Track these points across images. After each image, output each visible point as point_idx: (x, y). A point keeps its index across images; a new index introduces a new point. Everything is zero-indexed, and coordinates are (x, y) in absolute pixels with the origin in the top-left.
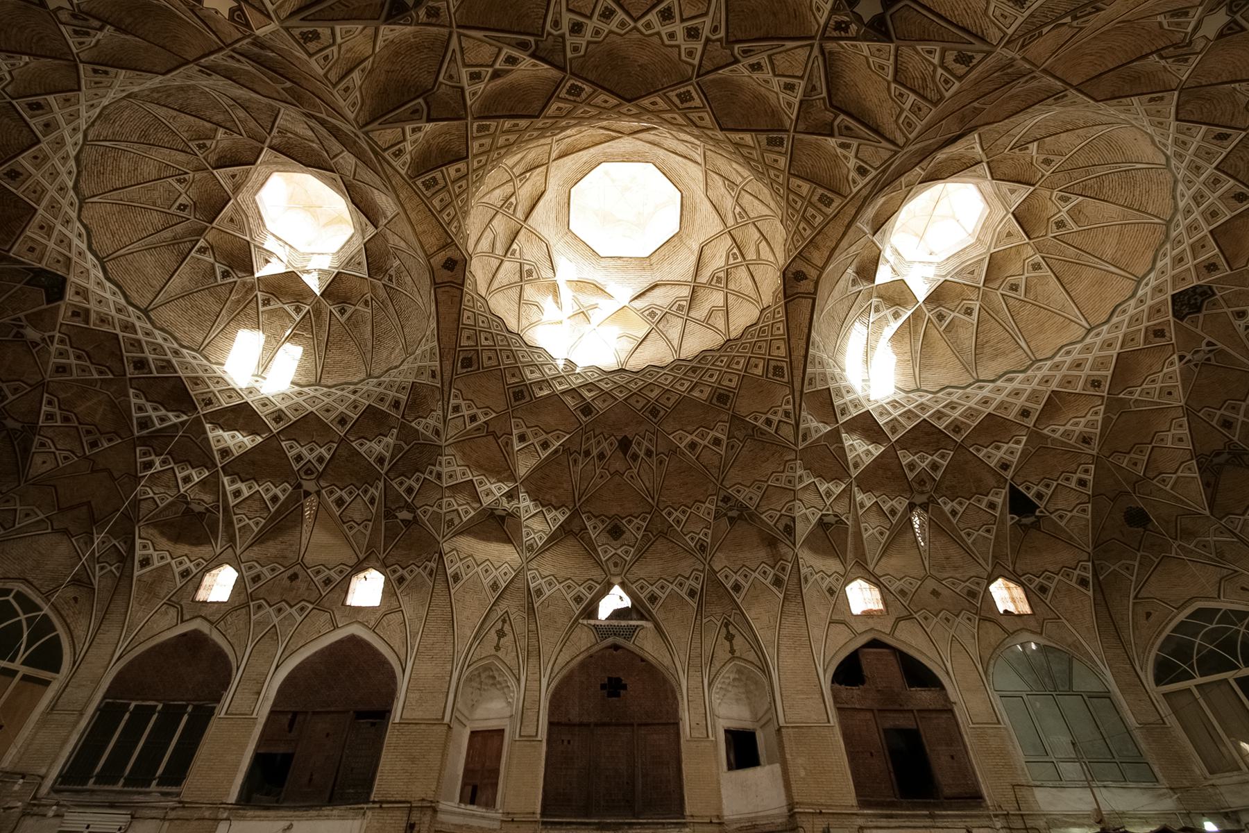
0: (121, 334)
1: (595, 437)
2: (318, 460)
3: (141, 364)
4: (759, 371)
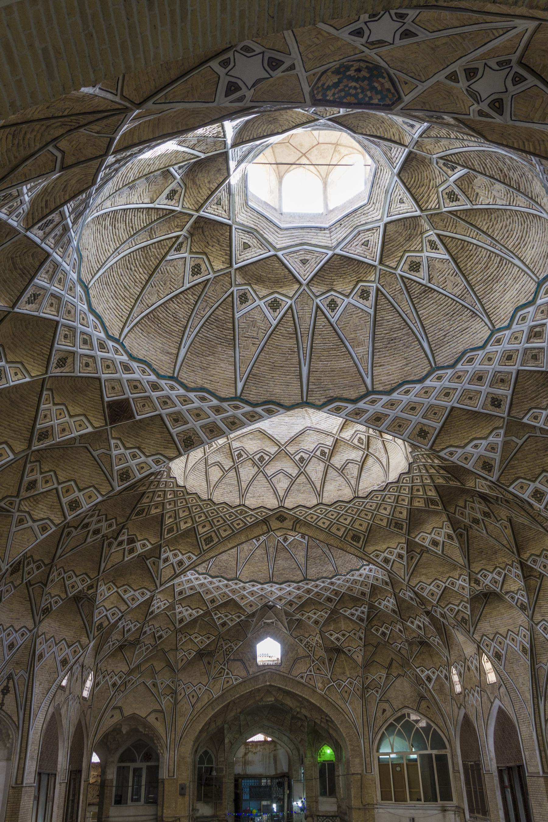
0: (310, 596)
1: (465, 508)
3: (329, 600)
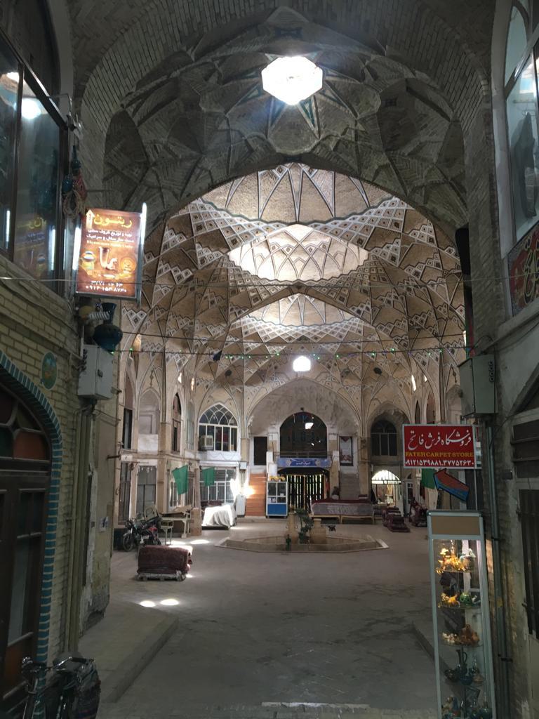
4: (252, 294)
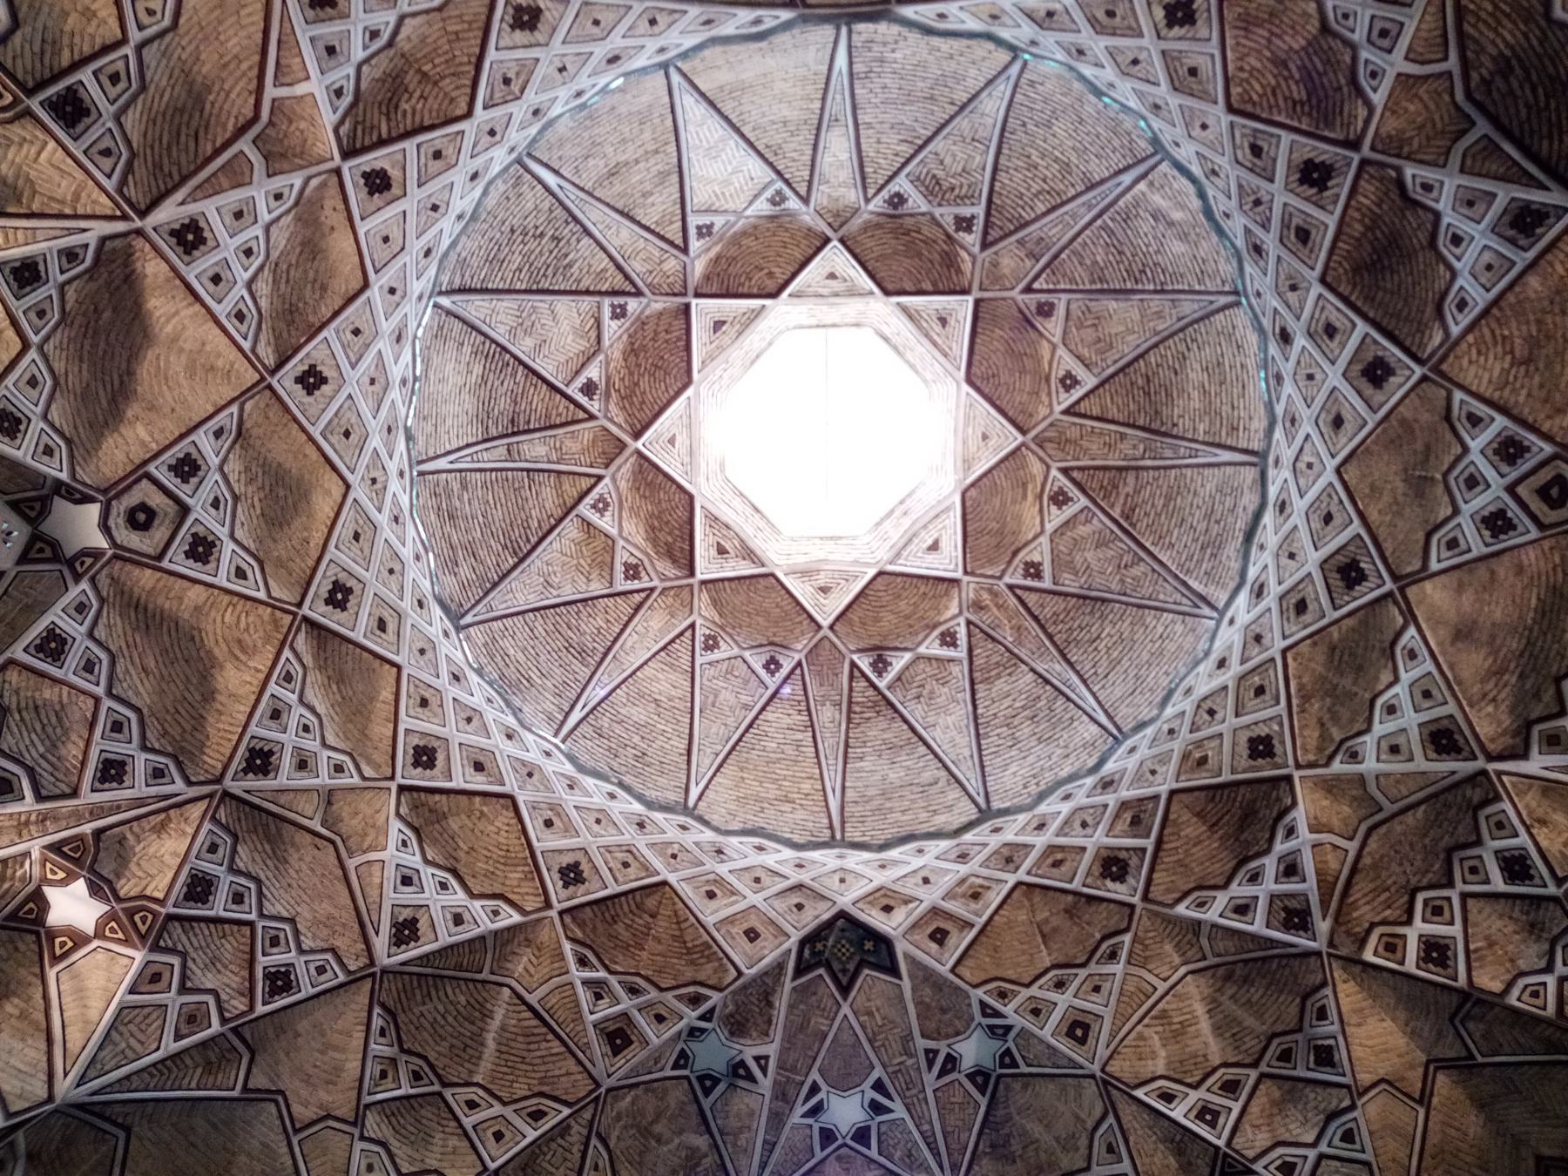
0: (1021, 875)
2: (1511, 460)
3: (1113, 865)
